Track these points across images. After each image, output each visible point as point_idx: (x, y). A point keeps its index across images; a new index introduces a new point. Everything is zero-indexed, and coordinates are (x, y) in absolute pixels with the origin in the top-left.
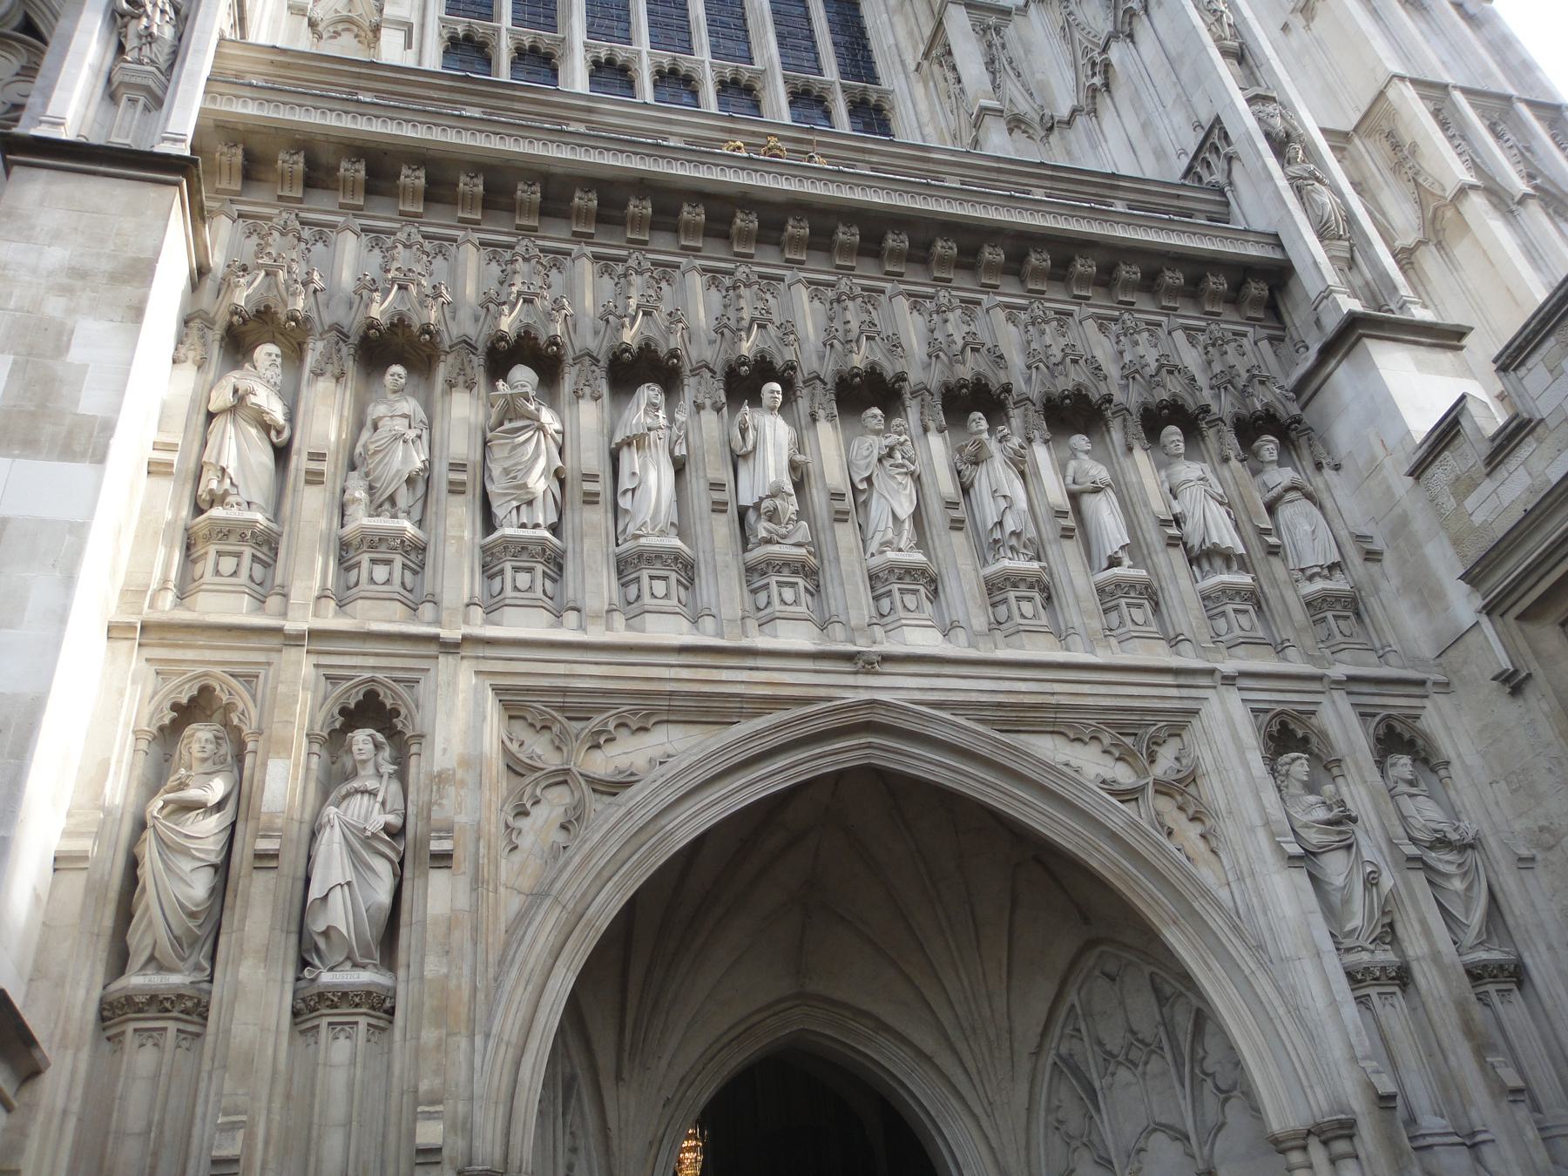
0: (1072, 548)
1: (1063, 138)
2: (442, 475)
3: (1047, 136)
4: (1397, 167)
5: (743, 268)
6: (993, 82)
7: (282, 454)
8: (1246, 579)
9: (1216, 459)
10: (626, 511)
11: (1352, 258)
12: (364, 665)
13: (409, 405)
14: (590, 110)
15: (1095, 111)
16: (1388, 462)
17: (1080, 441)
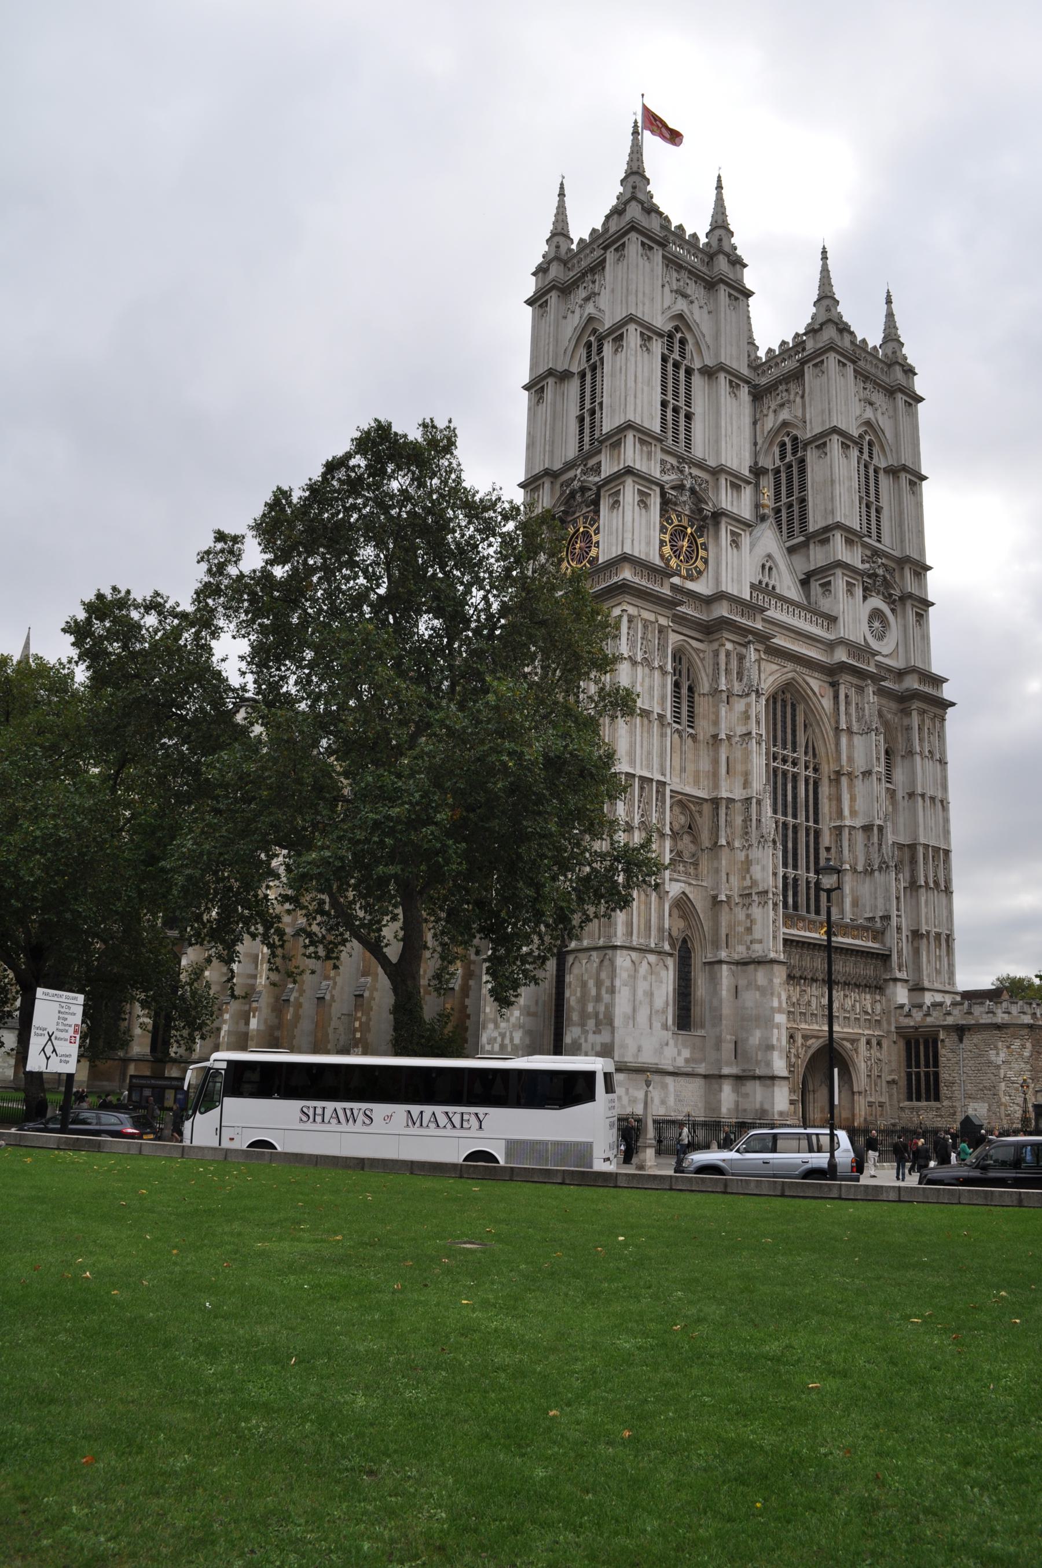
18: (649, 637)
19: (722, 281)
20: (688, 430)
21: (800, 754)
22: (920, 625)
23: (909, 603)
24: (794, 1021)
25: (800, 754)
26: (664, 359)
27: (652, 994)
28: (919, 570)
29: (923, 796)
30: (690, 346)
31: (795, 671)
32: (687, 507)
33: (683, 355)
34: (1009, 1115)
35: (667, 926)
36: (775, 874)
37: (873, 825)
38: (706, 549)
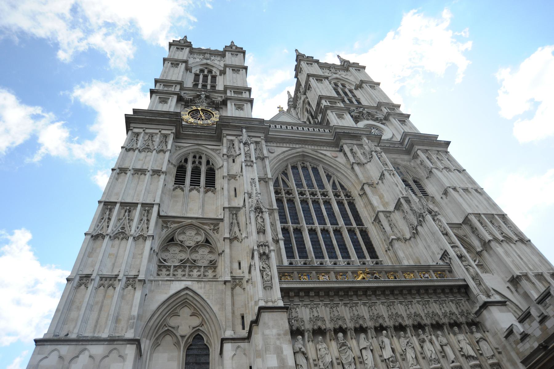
0: (445, 359)
1: (409, 243)
2: (335, 362)
3: (405, 242)
4: (473, 232)
5: (370, 302)
6: (392, 229)
7: (307, 359)
8: (477, 362)
9: (465, 333)
10: (367, 364)
11: (480, 282)
13: (324, 345)
14: (334, 268)
15: (415, 237)
16: (499, 333)
17: (439, 333)
18: (154, 140)
22: (406, 125)
23: (391, 118)
26: (197, 76)
32: (204, 103)
35: (135, 312)
36: (261, 231)
37: (399, 199)
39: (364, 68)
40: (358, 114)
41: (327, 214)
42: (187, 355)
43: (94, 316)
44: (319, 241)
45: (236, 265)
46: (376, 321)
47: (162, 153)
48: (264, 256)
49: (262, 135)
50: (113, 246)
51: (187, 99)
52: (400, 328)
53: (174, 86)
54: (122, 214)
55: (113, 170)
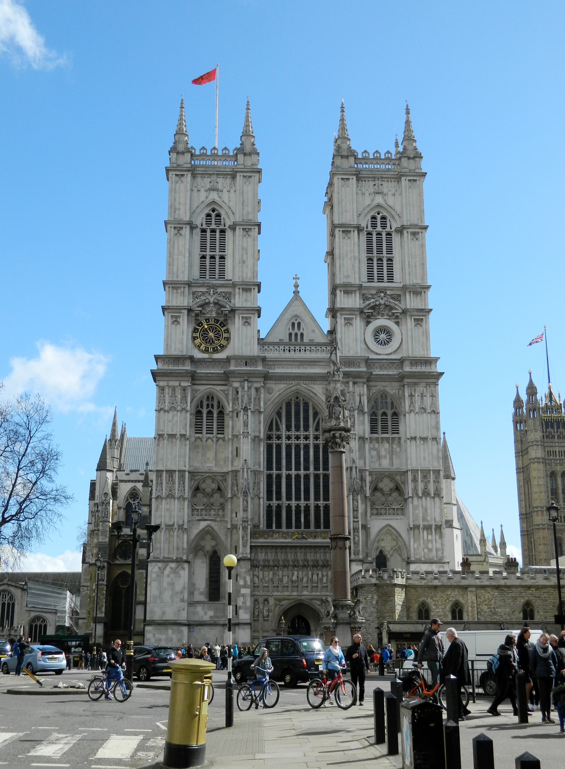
7: (258, 578)
12: (266, 597)
13: (267, 573)
18: (176, 395)
19: (237, 172)
20: (222, 265)
21: (311, 432)
22: (421, 325)
24: (268, 591)
25: (311, 432)
26: (204, 231)
27: (173, 584)
28: (419, 290)
29: (415, 438)
30: (223, 215)
31: (298, 385)
33: (218, 223)
34: (365, 641)
35: (185, 546)
36: (245, 510)
38: (228, 332)
39: (424, 175)
40: (372, 311)
41: (304, 458)
42: (210, 561)
43: (167, 546)
44: (291, 485)
45: (234, 515)
46: (294, 563)
47: (184, 412)
48: (245, 528)
49: (262, 379)
50: (167, 504)
51: (197, 312)
52: (304, 566)
53: (182, 290)
54: (168, 480)
55: (155, 438)
